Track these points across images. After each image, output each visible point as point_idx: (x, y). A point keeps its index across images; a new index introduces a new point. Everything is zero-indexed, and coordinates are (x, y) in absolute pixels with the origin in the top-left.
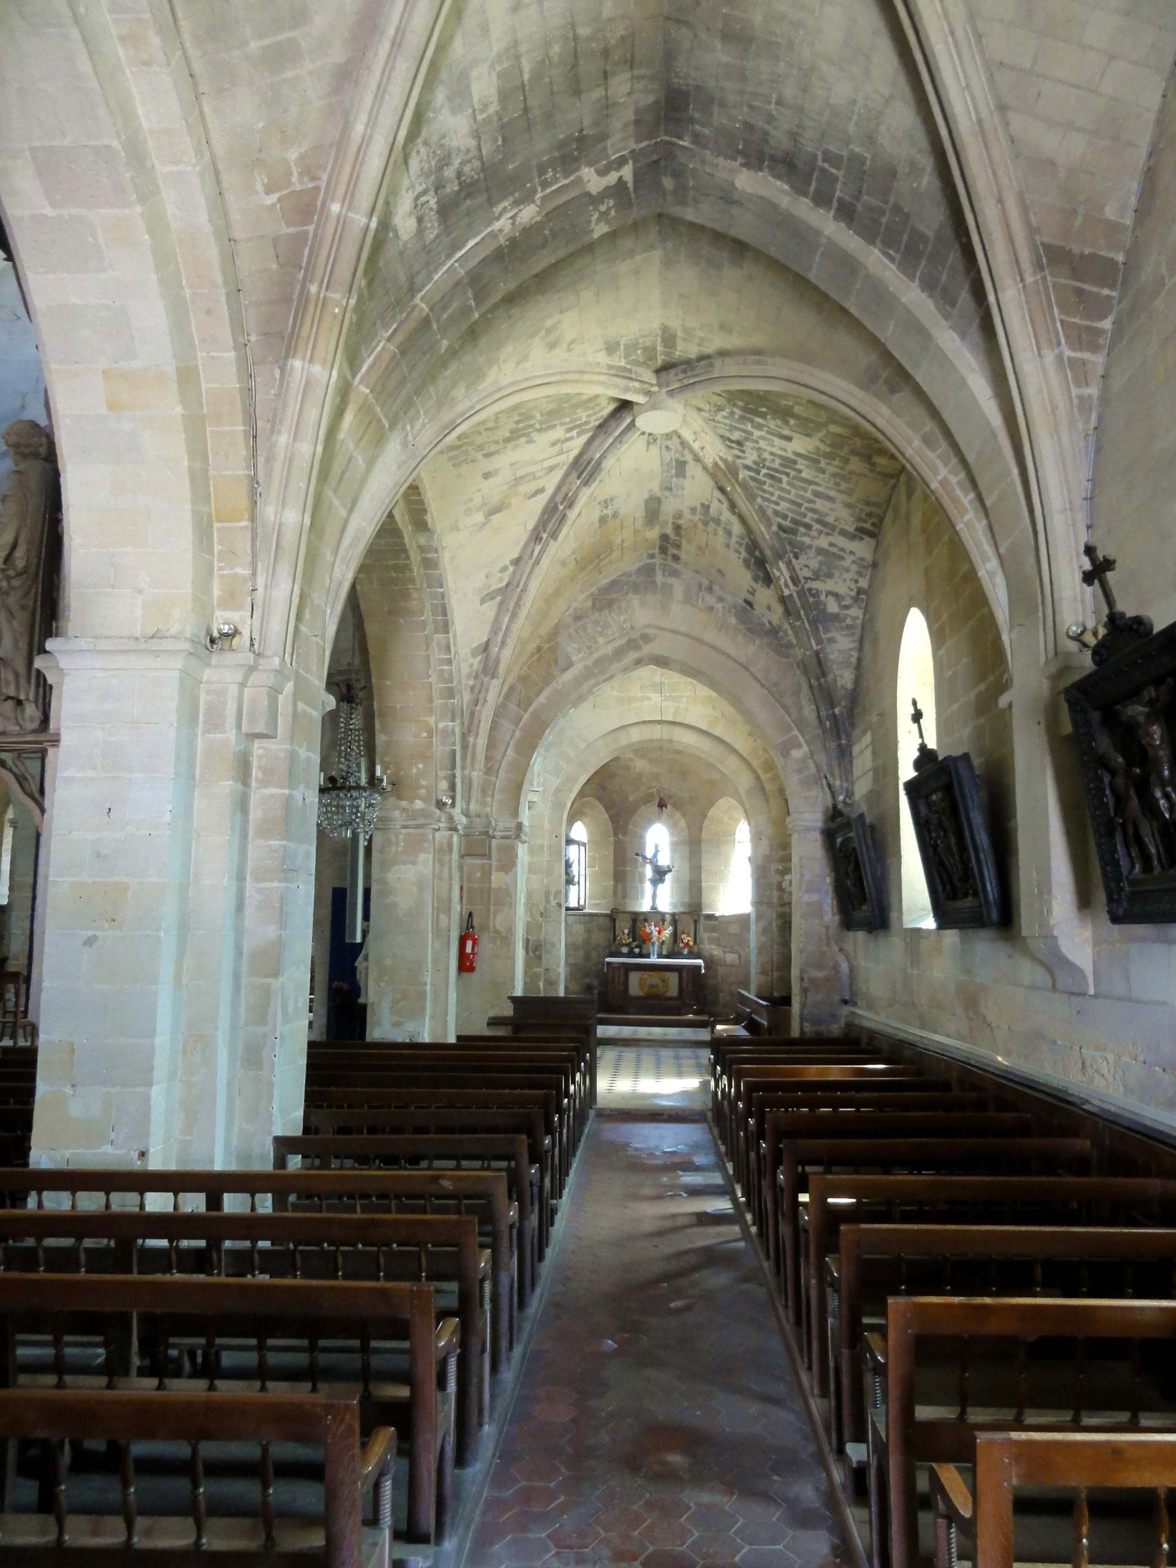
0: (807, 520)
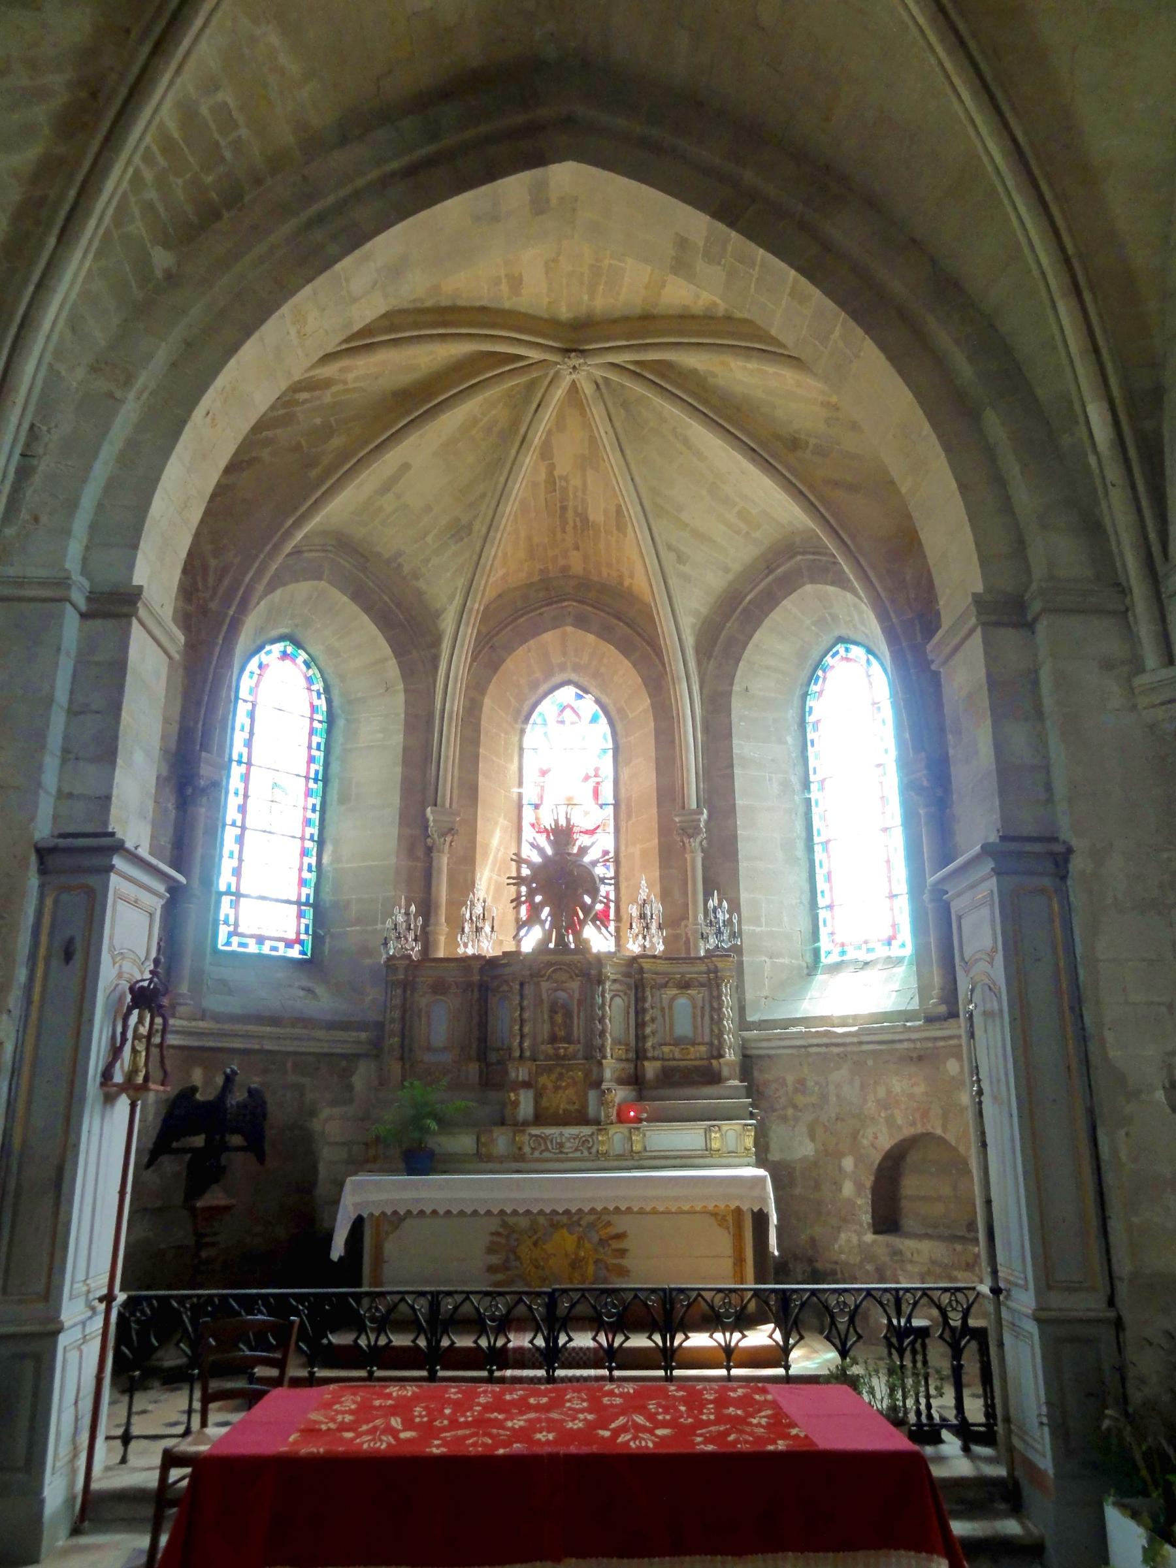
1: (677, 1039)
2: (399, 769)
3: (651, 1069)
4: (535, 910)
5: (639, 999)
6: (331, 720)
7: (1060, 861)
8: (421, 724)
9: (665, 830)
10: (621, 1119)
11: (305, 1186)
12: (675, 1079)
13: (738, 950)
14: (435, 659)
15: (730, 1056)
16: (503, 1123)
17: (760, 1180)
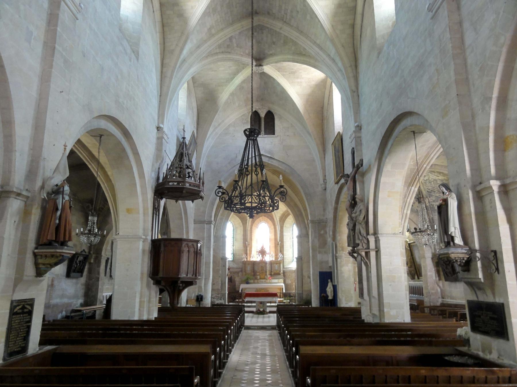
3: (272, 273)
7: (302, 259)
8: (245, 231)
9: (275, 244)
11: (235, 285)
12: (275, 274)
15: (282, 272)
16: (256, 279)
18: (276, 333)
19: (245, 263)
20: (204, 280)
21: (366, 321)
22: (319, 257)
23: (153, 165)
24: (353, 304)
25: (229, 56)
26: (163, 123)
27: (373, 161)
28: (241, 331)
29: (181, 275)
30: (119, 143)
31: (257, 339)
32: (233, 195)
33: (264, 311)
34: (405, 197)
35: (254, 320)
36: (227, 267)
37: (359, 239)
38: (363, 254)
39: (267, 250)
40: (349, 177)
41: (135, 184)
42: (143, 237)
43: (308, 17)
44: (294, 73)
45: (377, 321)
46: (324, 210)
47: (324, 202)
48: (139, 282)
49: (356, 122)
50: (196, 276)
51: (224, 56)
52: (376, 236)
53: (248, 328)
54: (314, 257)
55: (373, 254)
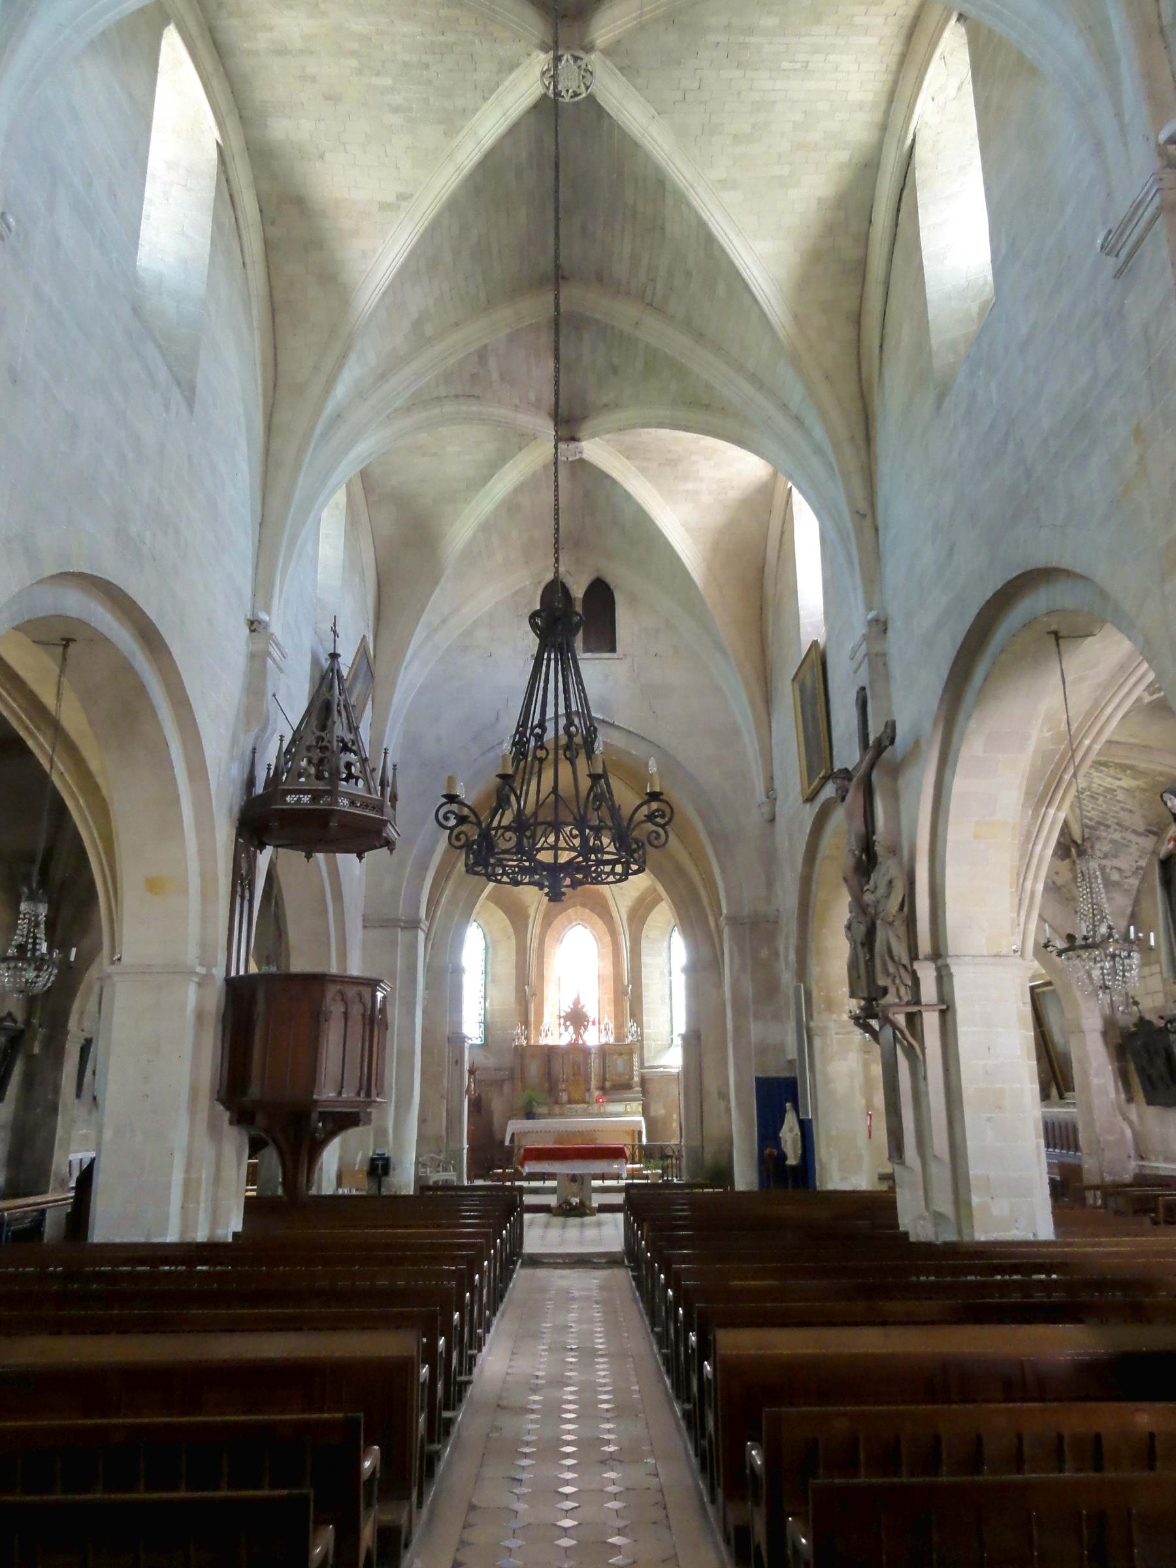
0: (1108, 823)
1: (616, 1073)
2: (514, 971)
3: (608, 1084)
4: (566, 1028)
5: (604, 1059)
6: (486, 949)
8: (522, 951)
9: (616, 991)
10: (597, 1101)
11: (490, 1124)
12: (615, 1088)
13: (641, 1041)
14: (526, 926)
15: (636, 1079)
16: (557, 1103)
17: (640, 1122)
18: (622, 1277)
19: (521, 1053)
20: (392, 1108)
21: (912, 1239)
22: (756, 1031)
23: (234, 741)
24: (862, 1181)
25: (475, 408)
26: (268, 609)
27: (927, 726)
28: (513, 1271)
29: (320, 1093)
30: (127, 668)
31: (566, 1297)
32: (495, 824)
33: (582, 1203)
34: (1029, 838)
35: (554, 1234)
36: (467, 1066)
37: (888, 974)
38: (901, 1020)
39: (591, 1011)
40: (850, 780)
41: (176, 800)
42: (199, 969)
43: (721, 290)
44: (672, 463)
45: (950, 1236)
46: (770, 884)
47: (769, 858)
48: (183, 1119)
49: (869, 608)
50: (368, 1094)
51: (464, 408)
52: (940, 962)
53: (535, 1261)
54: (740, 1031)
55: (931, 1021)
